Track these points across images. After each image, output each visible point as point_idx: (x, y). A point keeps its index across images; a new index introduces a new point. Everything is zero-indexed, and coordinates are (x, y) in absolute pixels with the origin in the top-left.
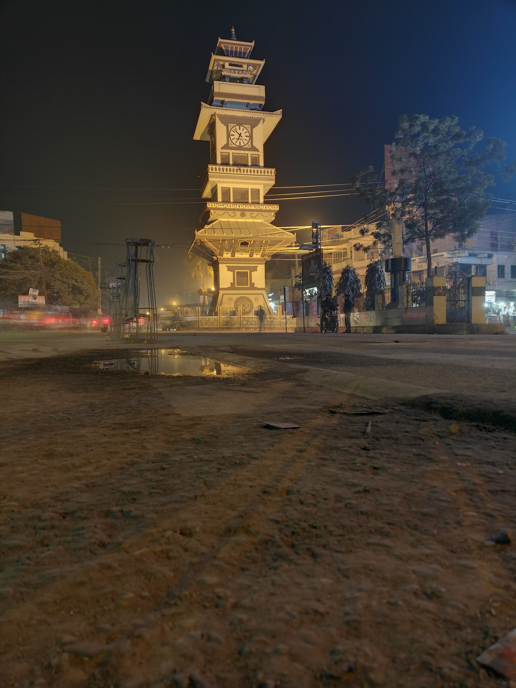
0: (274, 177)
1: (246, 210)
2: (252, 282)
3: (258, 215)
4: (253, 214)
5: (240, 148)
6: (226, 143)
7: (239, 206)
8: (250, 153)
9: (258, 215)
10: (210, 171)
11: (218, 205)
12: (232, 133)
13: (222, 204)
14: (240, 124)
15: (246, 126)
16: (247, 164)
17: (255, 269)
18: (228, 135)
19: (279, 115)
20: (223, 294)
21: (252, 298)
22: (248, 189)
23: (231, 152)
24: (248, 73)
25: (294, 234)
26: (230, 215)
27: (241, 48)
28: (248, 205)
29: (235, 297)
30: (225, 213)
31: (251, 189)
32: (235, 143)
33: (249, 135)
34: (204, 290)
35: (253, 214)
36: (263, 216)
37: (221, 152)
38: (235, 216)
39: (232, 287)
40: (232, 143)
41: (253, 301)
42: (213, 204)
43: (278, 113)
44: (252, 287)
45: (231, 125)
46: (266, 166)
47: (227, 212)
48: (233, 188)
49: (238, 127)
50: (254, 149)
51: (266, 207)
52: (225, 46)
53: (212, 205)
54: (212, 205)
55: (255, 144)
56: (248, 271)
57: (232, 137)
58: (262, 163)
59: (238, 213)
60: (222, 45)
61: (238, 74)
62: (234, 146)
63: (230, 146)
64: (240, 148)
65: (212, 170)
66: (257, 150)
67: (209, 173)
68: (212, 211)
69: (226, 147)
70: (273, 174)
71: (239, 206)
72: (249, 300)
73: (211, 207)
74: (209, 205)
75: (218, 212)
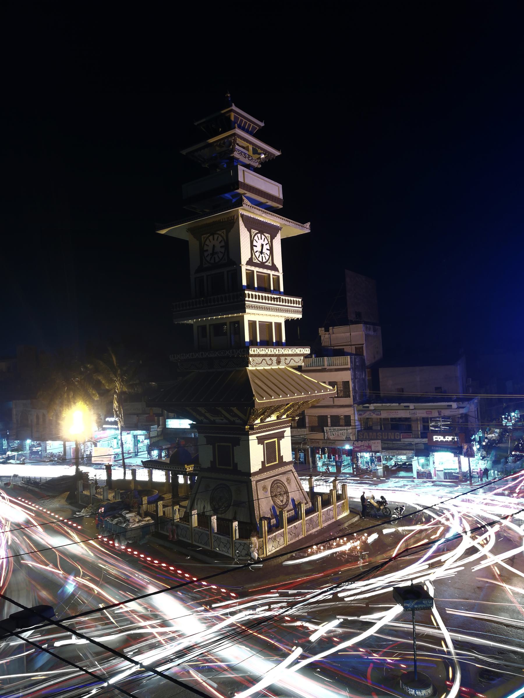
0: (301, 309)
1: (283, 355)
2: (281, 455)
3: (291, 360)
4: (287, 359)
5: (262, 265)
6: (250, 257)
7: (279, 350)
8: (272, 273)
9: (290, 362)
10: (247, 299)
11: (260, 351)
12: (255, 243)
13: (263, 349)
14: (261, 232)
15: (267, 235)
16: (266, 286)
17: (281, 436)
18: (252, 246)
19: (308, 229)
20: (256, 482)
21: (283, 479)
22: (271, 323)
23: (256, 269)
24: (257, 162)
25: (334, 387)
26: (267, 363)
27: (249, 125)
28: (286, 349)
29: (268, 483)
30: (262, 361)
31: (275, 323)
32: (258, 258)
33: (269, 248)
34: (189, 469)
35: (287, 359)
36: (295, 361)
37: (246, 270)
38: (272, 363)
39: (264, 469)
40: (255, 258)
41: (286, 484)
42: (255, 349)
43: (307, 227)
44: (282, 464)
45: (254, 231)
46: (286, 293)
47: (265, 360)
48: (259, 322)
49: (259, 235)
50: (274, 268)
51: (300, 351)
52: (235, 117)
53: (254, 351)
54: (254, 351)
55: (276, 262)
56: (276, 440)
57: (255, 249)
58: (282, 289)
59: (274, 359)
60: (233, 115)
61: (249, 159)
62: (256, 261)
63: (254, 261)
64: (262, 265)
65: (249, 297)
66: (276, 269)
67: (246, 302)
68: (251, 359)
69: (250, 262)
70: (300, 306)
71: (279, 350)
72: (283, 484)
73: (253, 353)
74: (251, 351)
75: (256, 359)
